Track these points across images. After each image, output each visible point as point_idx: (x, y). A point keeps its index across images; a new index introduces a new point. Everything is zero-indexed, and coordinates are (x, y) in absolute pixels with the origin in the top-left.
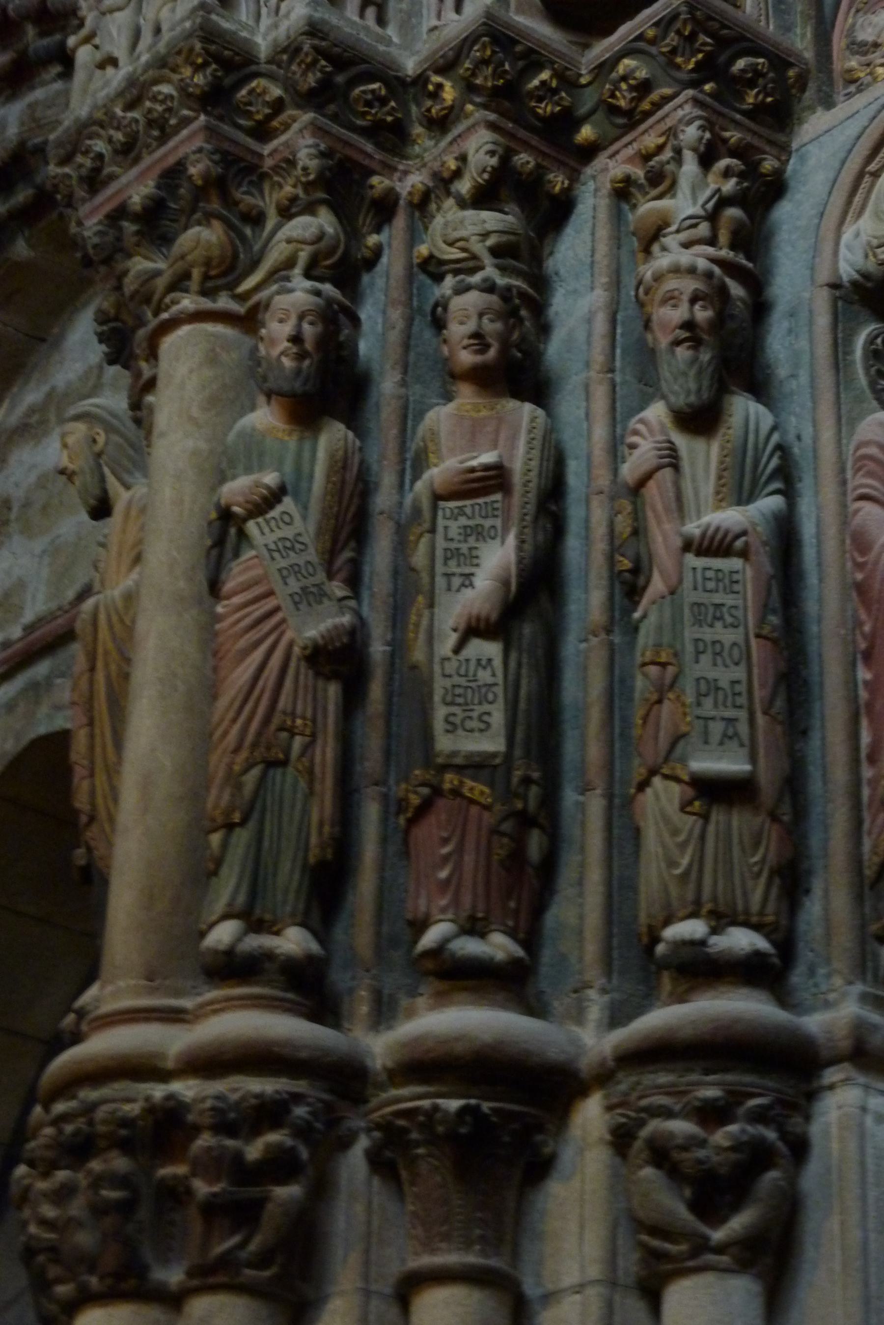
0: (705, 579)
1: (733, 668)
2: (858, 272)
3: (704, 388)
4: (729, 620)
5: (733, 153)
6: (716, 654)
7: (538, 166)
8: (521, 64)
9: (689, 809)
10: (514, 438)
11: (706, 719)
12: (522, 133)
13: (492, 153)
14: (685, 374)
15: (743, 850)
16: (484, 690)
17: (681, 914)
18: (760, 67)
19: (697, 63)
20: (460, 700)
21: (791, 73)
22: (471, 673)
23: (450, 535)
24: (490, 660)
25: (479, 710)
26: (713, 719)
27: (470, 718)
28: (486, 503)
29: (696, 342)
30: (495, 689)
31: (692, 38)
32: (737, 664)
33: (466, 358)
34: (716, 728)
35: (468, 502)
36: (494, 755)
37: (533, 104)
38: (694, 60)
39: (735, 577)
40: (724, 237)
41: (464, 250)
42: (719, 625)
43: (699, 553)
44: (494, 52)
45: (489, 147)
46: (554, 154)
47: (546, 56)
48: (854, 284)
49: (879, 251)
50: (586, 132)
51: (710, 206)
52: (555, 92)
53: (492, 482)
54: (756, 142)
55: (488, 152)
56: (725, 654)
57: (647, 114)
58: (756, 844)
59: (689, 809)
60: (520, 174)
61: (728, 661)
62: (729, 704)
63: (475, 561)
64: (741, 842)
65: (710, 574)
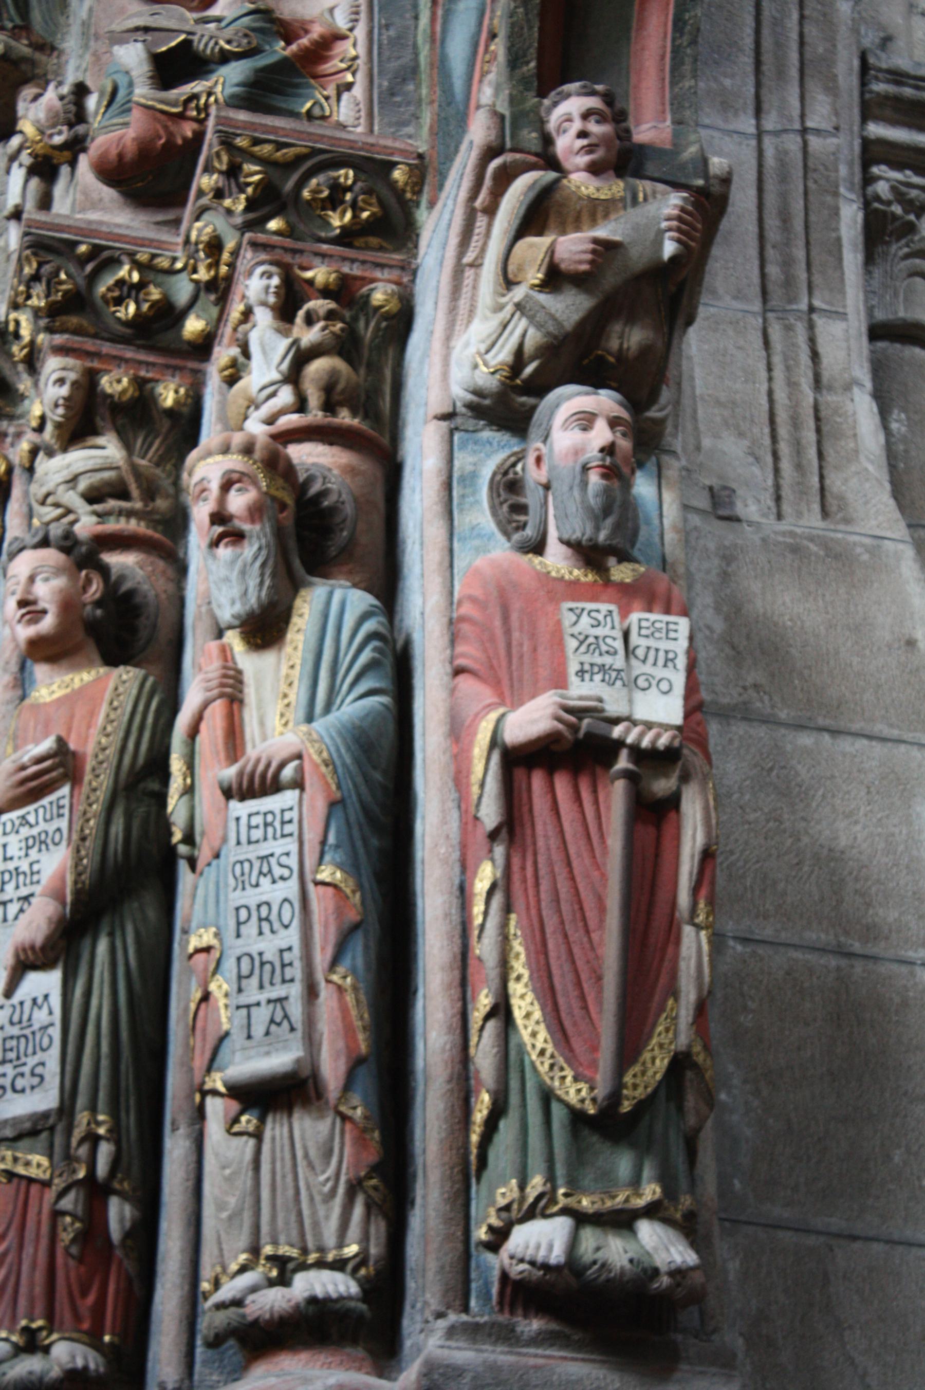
0: (250, 827)
1: (283, 933)
2: (466, 390)
3: (251, 590)
4: (278, 871)
5: (326, 292)
6: (260, 919)
7: (140, 383)
8: (89, 268)
9: (236, 1129)
10: (92, 714)
11: (248, 1007)
12: (107, 348)
13: (61, 381)
14: (227, 580)
15: (311, 1166)
16: (38, 1036)
17: (234, 1267)
18: (342, 180)
19: (248, 199)
20: (12, 1055)
21: (398, 174)
22: (25, 1017)
23: (9, 855)
24: (46, 997)
25: (31, 1061)
26: (258, 1004)
27: (22, 1075)
28: (51, 803)
29: (238, 537)
30: (51, 1031)
31: (233, 172)
32: (286, 927)
33: (25, 632)
34: (261, 1016)
35: (31, 808)
36: (45, 1115)
37: (114, 309)
38: (243, 196)
39: (287, 816)
40: (314, 399)
41: (57, 505)
42: (265, 882)
43: (243, 798)
44: (40, 265)
45: (55, 376)
46: (160, 360)
47: (119, 249)
48: (470, 406)
49: (488, 357)
50: (193, 325)
51: (285, 366)
52: (141, 285)
53: (54, 774)
54: (356, 270)
55: (56, 382)
56: (274, 917)
57: (229, 279)
58: (328, 1154)
59: (236, 1129)
60: (111, 396)
61: (276, 925)
62: (278, 978)
63: (35, 878)
64: (306, 1155)
65: (256, 820)
